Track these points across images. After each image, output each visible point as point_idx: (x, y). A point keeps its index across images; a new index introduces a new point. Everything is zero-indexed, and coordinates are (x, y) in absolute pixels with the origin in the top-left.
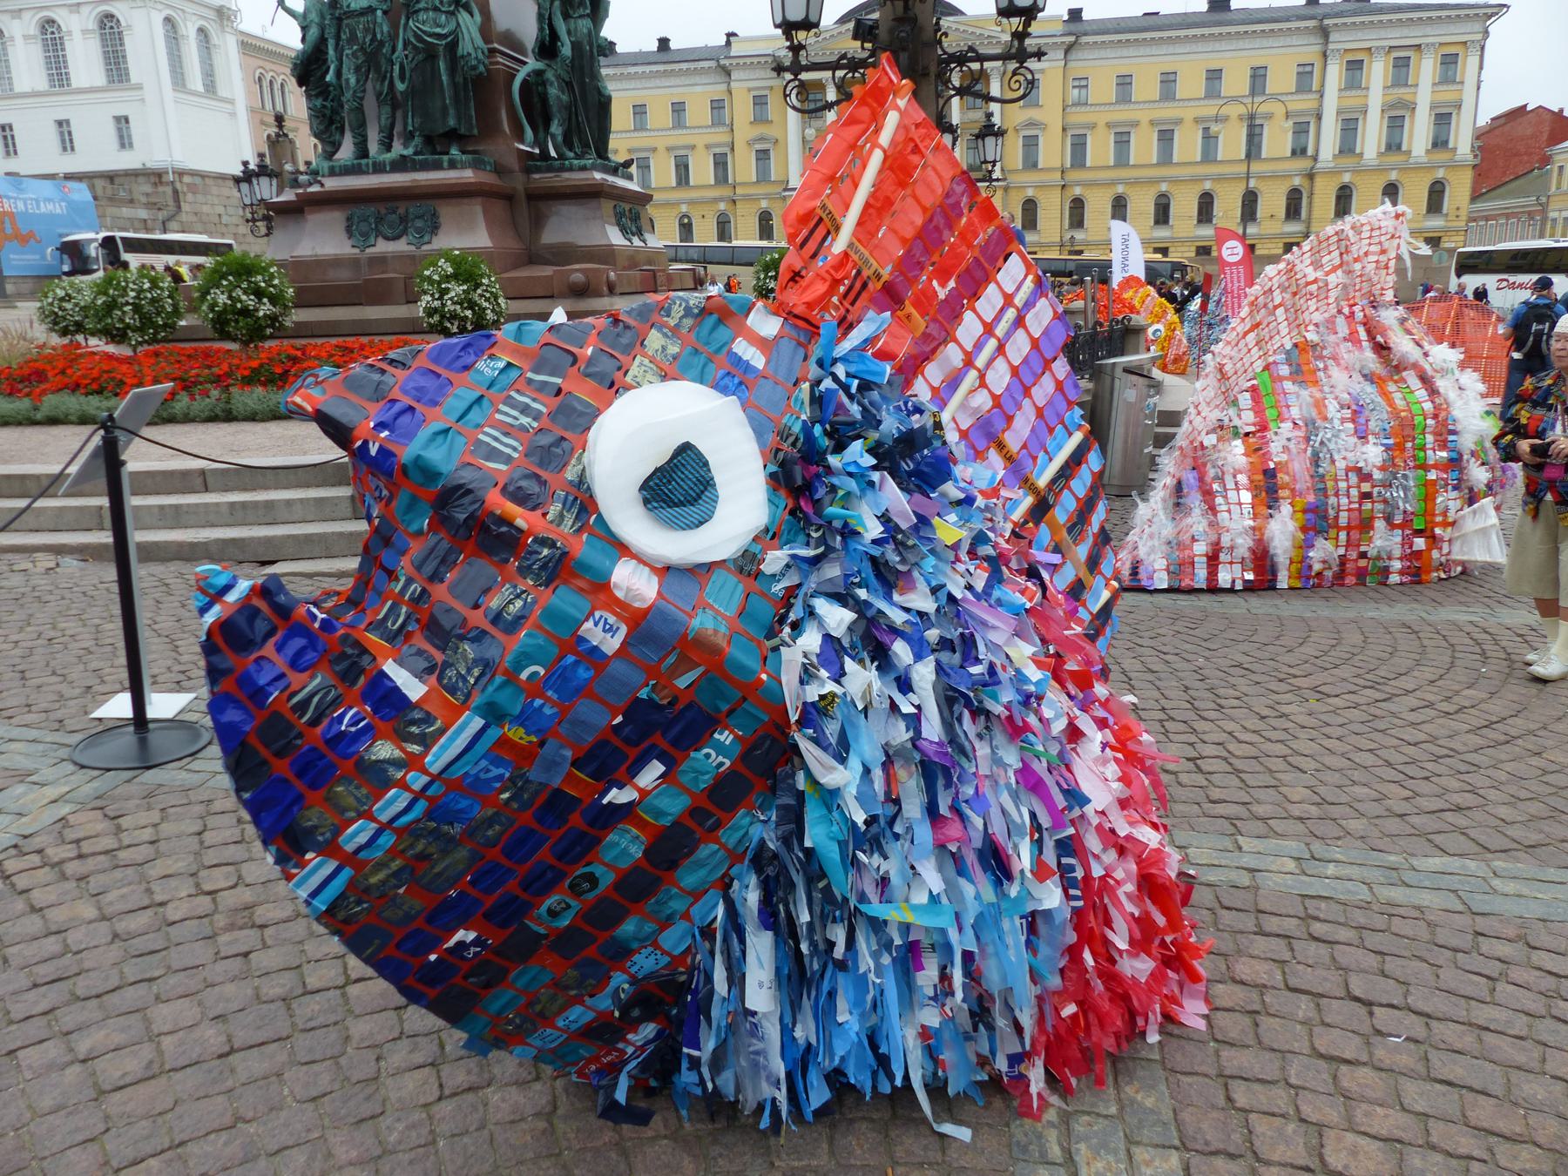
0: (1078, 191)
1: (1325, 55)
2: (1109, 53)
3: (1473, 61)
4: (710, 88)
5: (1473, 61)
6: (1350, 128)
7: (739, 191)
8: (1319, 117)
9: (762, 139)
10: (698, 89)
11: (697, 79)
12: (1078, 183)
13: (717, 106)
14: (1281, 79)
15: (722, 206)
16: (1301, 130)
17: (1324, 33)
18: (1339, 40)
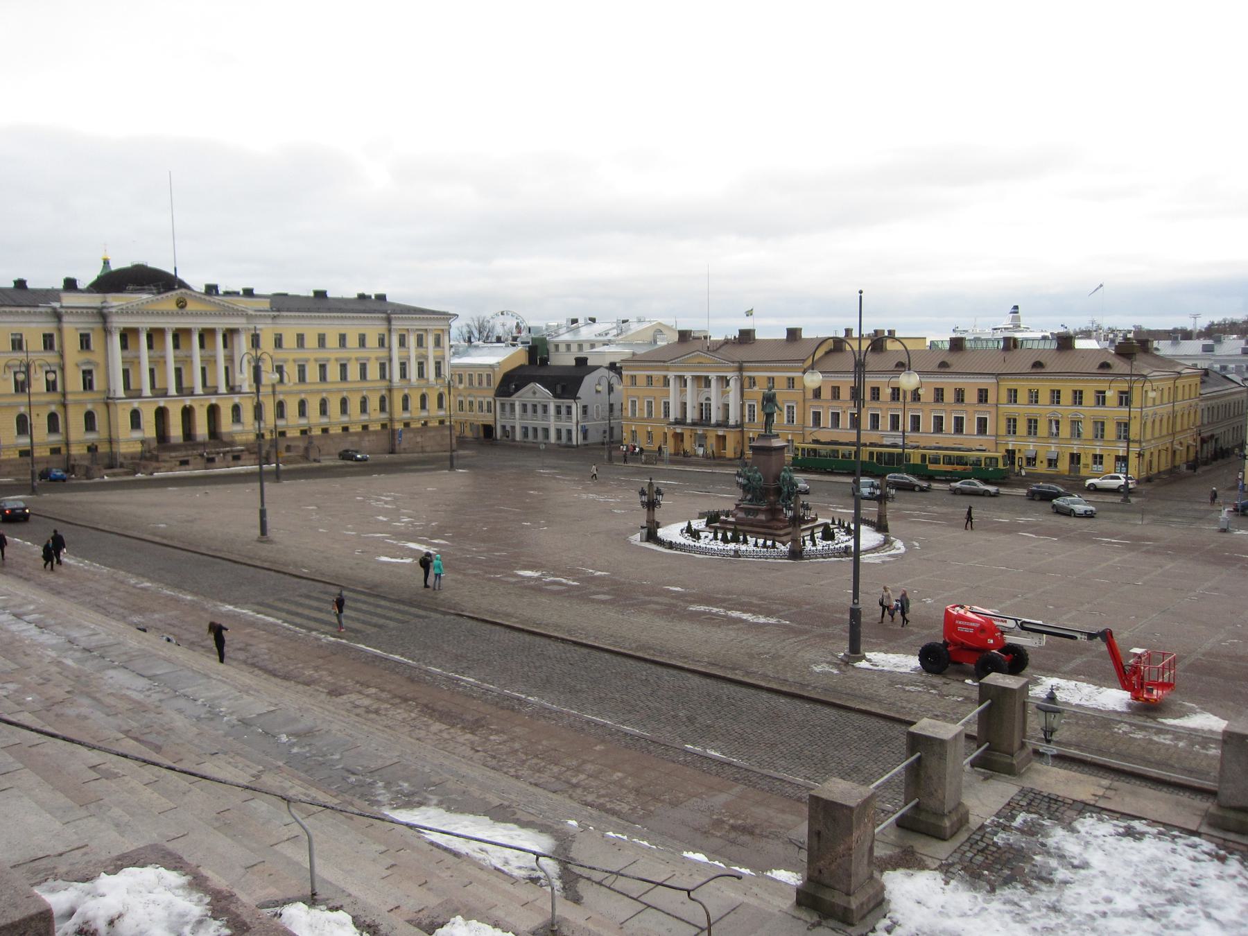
0: (281, 397)
1: (390, 331)
2: (292, 321)
3: (447, 338)
4: (40, 325)
5: (447, 338)
6: (403, 366)
7: (70, 397)
8: (390, 360)
9: (89, 363)
10: (33, 325)
11: (33, 319)
12: (281, 393)
13: (48, 341)
14: (372, 341)
15: (53, 408)
16: (382, 366)
17: (389, 320)
18: (396, 325)
